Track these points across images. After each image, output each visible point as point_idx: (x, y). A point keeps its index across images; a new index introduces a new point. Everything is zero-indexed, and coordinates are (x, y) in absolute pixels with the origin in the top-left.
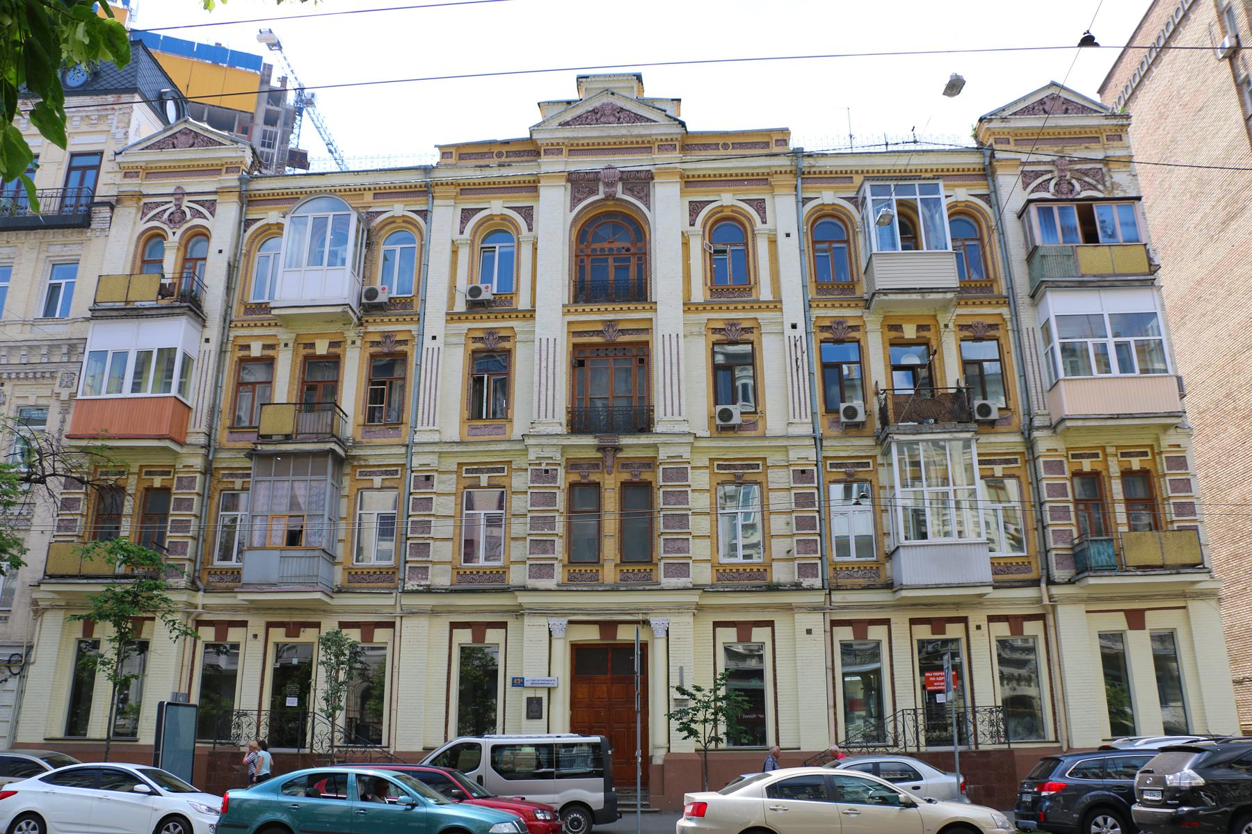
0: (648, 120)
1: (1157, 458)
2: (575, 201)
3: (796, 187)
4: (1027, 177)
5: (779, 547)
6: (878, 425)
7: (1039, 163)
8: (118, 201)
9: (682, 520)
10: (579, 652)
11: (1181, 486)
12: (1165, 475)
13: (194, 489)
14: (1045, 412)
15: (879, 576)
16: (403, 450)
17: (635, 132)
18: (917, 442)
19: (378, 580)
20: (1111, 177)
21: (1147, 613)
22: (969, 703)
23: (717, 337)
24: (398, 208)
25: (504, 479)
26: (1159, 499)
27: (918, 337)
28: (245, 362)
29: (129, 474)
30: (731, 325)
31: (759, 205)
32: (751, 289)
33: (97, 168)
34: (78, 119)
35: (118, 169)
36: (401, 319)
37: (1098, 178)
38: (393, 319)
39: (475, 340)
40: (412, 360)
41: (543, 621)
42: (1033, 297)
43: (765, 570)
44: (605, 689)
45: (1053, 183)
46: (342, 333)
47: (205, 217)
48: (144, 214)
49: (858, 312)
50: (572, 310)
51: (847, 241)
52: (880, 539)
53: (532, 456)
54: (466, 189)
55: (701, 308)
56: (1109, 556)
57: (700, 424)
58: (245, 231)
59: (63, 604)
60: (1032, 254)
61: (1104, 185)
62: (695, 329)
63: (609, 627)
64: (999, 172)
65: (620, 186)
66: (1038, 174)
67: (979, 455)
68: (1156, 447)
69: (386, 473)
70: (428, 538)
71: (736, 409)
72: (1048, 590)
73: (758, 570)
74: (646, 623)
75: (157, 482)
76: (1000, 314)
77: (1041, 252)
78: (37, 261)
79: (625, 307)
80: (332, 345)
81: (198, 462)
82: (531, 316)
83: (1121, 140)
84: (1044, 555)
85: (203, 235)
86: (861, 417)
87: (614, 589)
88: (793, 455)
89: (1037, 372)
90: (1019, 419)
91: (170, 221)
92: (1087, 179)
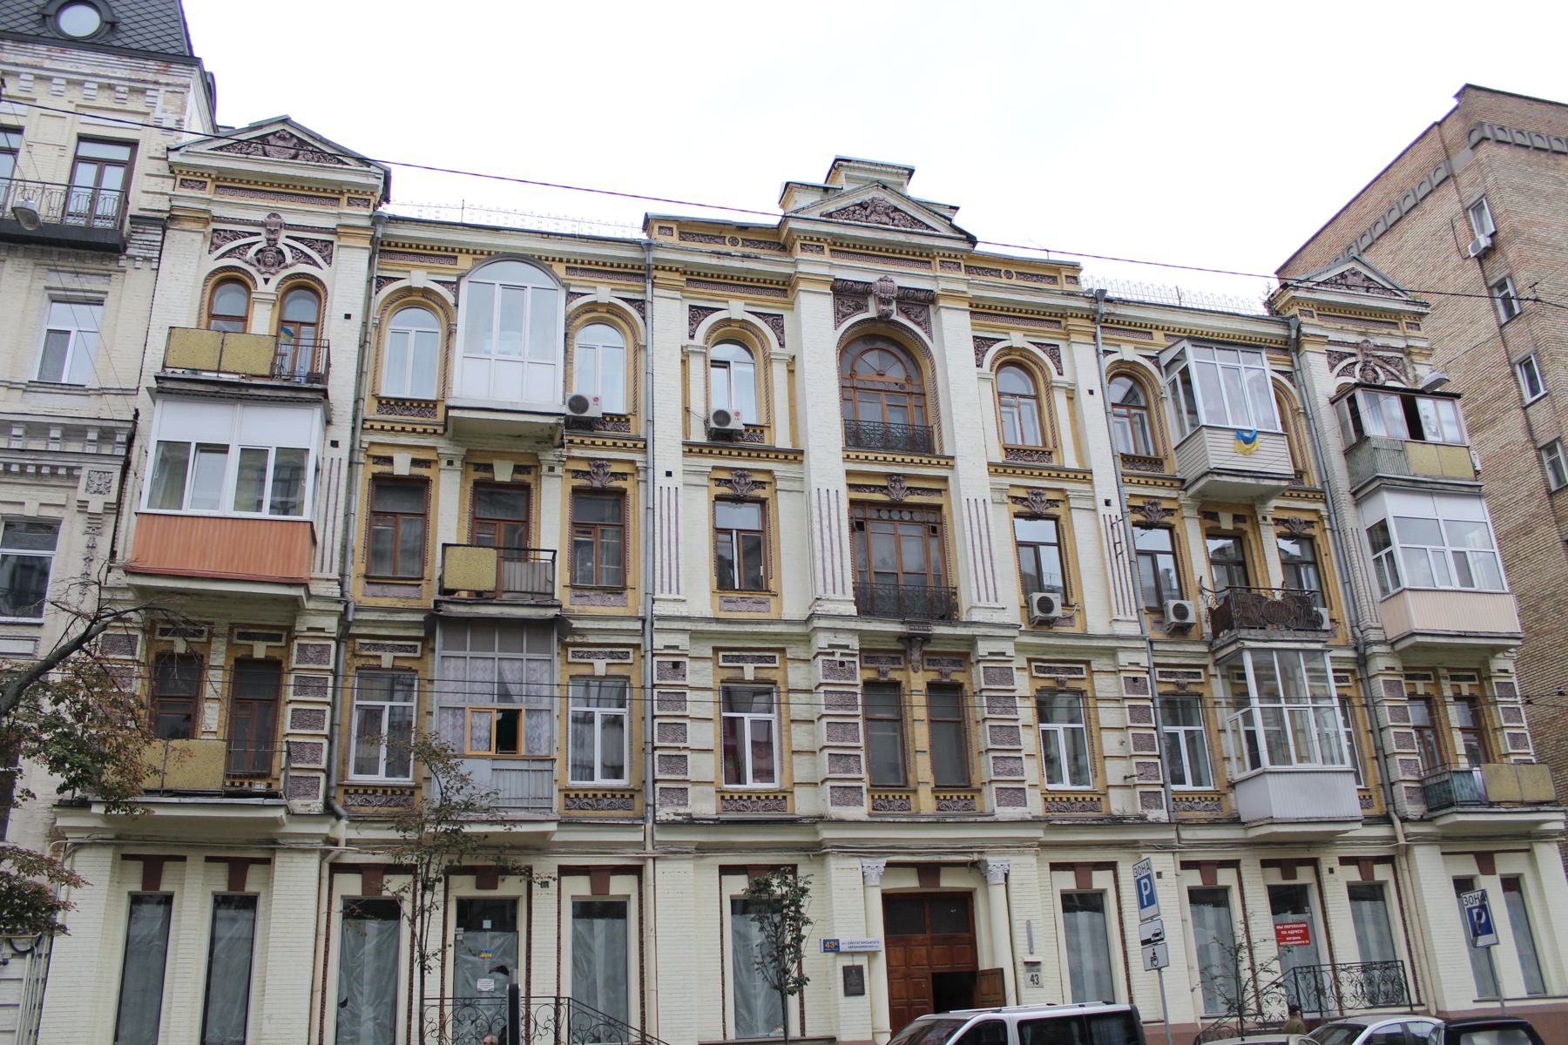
0: (928, 227)
1: (1485, 683)
2: (840, 316)
3: (1095, 337)
4: (1334, 358)
5: (1115, 772)
6: (1207, 629)
7: (1343, 344)
8: (173, 218)
9: (1012, 733)
10: (890, 900)
11: (1513, 715)
12: (1496, 703)
13: (328, 664)
14: (1379, 625)
15: (1221, 809)
16: (638, 625)
17: (916, 240)
18: (1272, 649)
19: (611, 807)
20: (1414, 369)
21: (1496, 856)
22: (1325, 959)
23: (1019, 508)
24: (604, 292)
25: (774, 671)
26: (1490, 729)
27: (1235, 529)
28: (384, 484)
29: (211, 635)
30: (1036, 495)
31: (1053, 351)
32: (1050, 453)
33: (128, 166)
34: (95, 86)
35: (167, 173)
36: (620, 443)
37: (1400, 368)
38: (609, 443)
39: (719, 482)
40: (637, 499)
41: (855, 863)
42: (1354, 494)
43: (1099, 799)
44: (924, 951)
45: (1358, 367)
46: (536, 455)
47: (315, 263)
48: (214, 246)
49: (1174, 494)
50: (853, 455)
51: (1146, 408)
52: (1219, 764)
53: (822, 640)
54: (696, 277)
55: (1001, 470)
56: (1471, 790)
57: (1014, 614)
58: (377, 293)
59: (111, 836)
60: (1357, 443)
61: (1407, 378)
62: (997, 497)
63: (928, 871)
64: (1307, 347)
65: (894, 307)
66: (1342, 356)
67: (1334, 671)
68: (1483, 672)
69: (611, 655)
70: (684, 748)
71: (1057, 599)
72: (1402, 827)
73: (1091, 799)
74: (977, 867)
75: (260, 650)
76: (1316, 511)
77: (1374, 444)
78: (29, 293)
79: (916, 460)
80: (518, 469)
81: (331, 624)
82: (795, 458)
83: (1419, 330)
84: (1387, 787)
85: (310, 288)
86: (1191, 619)
87: (938, 823)
88: (1124, 659)
89: (1365, 579)
90: (1344, 631)
91: (258, 261)
92: (1389, 367)
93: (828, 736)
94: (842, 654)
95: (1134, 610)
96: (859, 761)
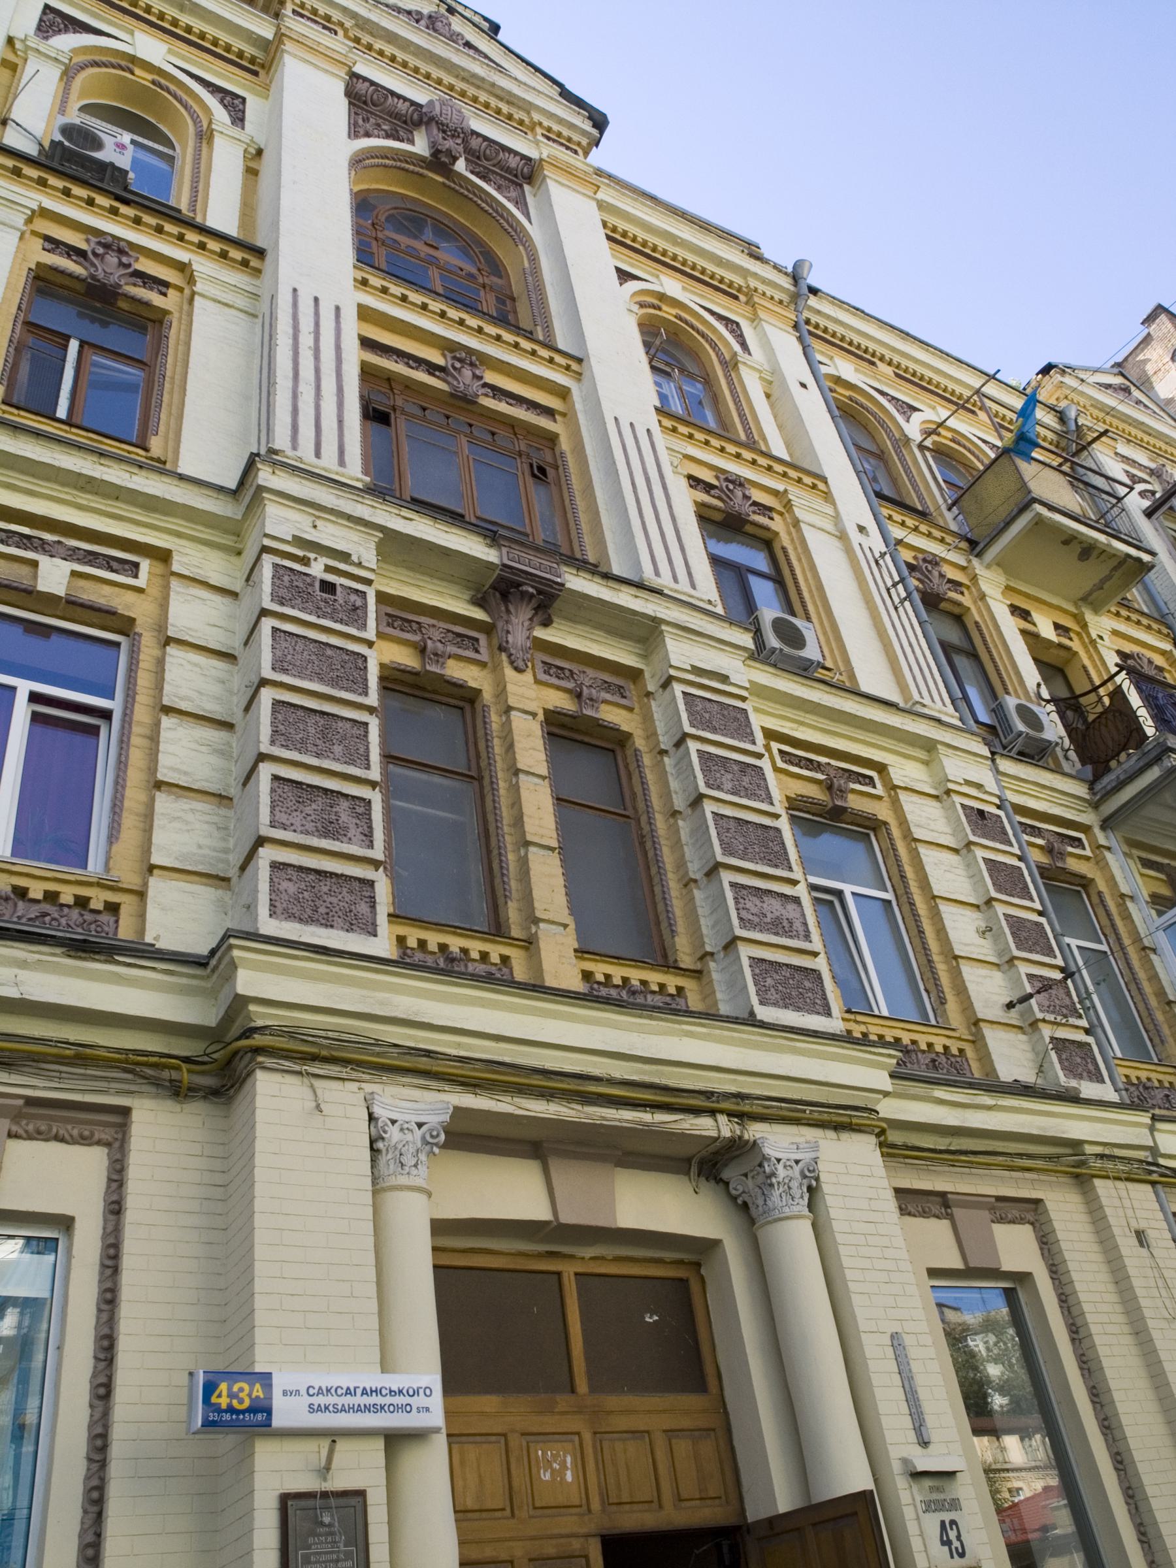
25: (130, 597)
39: (53, 244)
93: (275, 732)
94: (328, 569)
95: (948, 701)
96: (368, 815)
